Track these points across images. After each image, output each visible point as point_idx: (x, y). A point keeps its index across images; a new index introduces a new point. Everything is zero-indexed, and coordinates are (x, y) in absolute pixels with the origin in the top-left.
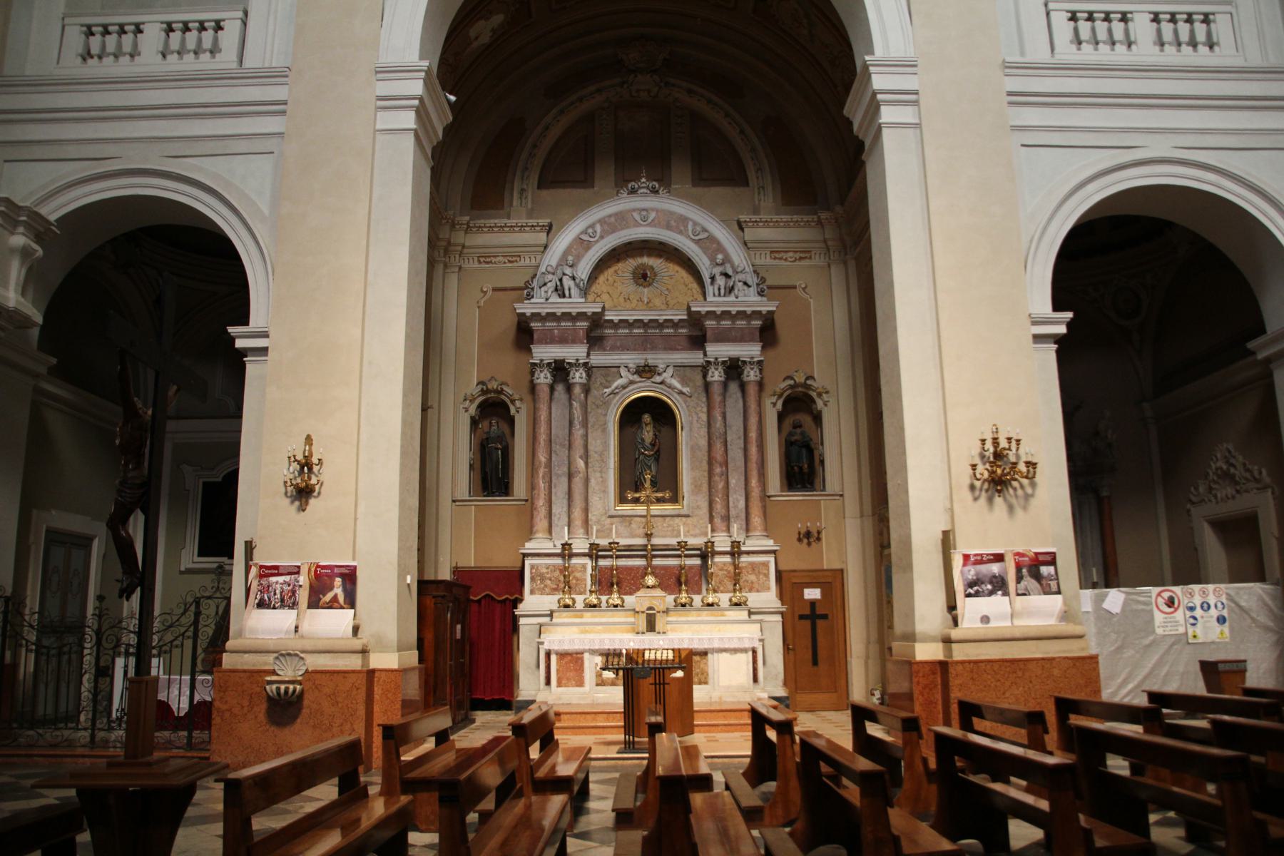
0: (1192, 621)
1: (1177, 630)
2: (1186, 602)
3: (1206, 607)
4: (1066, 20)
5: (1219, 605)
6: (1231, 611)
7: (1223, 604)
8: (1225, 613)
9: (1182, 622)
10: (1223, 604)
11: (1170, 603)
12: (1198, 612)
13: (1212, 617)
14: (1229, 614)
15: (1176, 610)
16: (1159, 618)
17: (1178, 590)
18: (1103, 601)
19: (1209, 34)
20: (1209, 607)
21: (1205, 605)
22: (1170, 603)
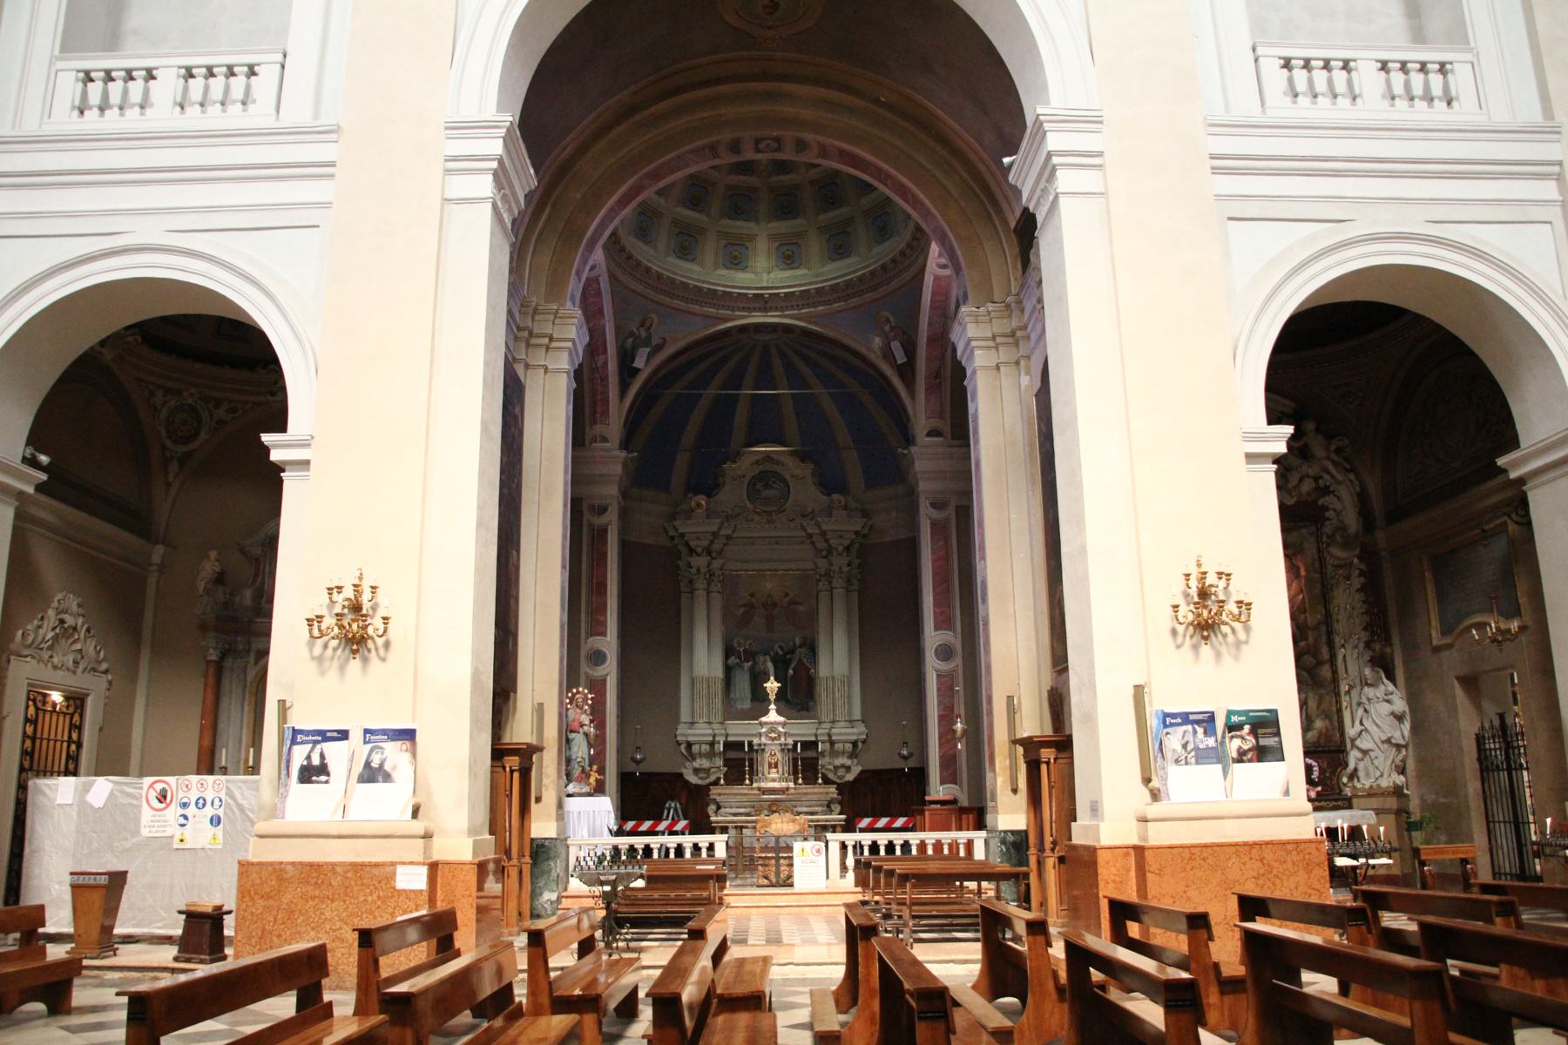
0: (182, 821)
1: (164, 831)
2: (180, 796)
3: (201, 803)
4: (260, 76)
5: (217, 802)
6: (228, 806)
7: (221, 800)
8: (221, 812)
9: (172, 821)
10: (221, 800)
11: (162, 797)
12: (191, 810)
13: (205, 816)
14: (225, 813)
15: (168, 806)
16: (147, 814)
17: (171, 780)
18: (88, 791)
19: (1350, 83)
20: (204, 805)
21: (201, 801)
22: (162, 797)
